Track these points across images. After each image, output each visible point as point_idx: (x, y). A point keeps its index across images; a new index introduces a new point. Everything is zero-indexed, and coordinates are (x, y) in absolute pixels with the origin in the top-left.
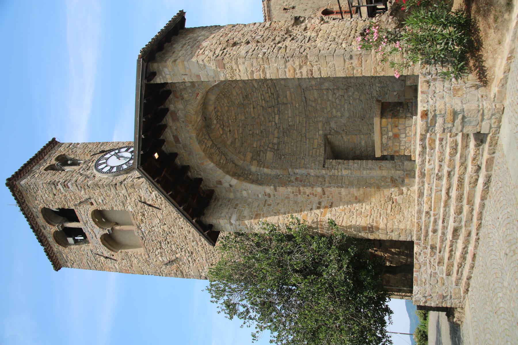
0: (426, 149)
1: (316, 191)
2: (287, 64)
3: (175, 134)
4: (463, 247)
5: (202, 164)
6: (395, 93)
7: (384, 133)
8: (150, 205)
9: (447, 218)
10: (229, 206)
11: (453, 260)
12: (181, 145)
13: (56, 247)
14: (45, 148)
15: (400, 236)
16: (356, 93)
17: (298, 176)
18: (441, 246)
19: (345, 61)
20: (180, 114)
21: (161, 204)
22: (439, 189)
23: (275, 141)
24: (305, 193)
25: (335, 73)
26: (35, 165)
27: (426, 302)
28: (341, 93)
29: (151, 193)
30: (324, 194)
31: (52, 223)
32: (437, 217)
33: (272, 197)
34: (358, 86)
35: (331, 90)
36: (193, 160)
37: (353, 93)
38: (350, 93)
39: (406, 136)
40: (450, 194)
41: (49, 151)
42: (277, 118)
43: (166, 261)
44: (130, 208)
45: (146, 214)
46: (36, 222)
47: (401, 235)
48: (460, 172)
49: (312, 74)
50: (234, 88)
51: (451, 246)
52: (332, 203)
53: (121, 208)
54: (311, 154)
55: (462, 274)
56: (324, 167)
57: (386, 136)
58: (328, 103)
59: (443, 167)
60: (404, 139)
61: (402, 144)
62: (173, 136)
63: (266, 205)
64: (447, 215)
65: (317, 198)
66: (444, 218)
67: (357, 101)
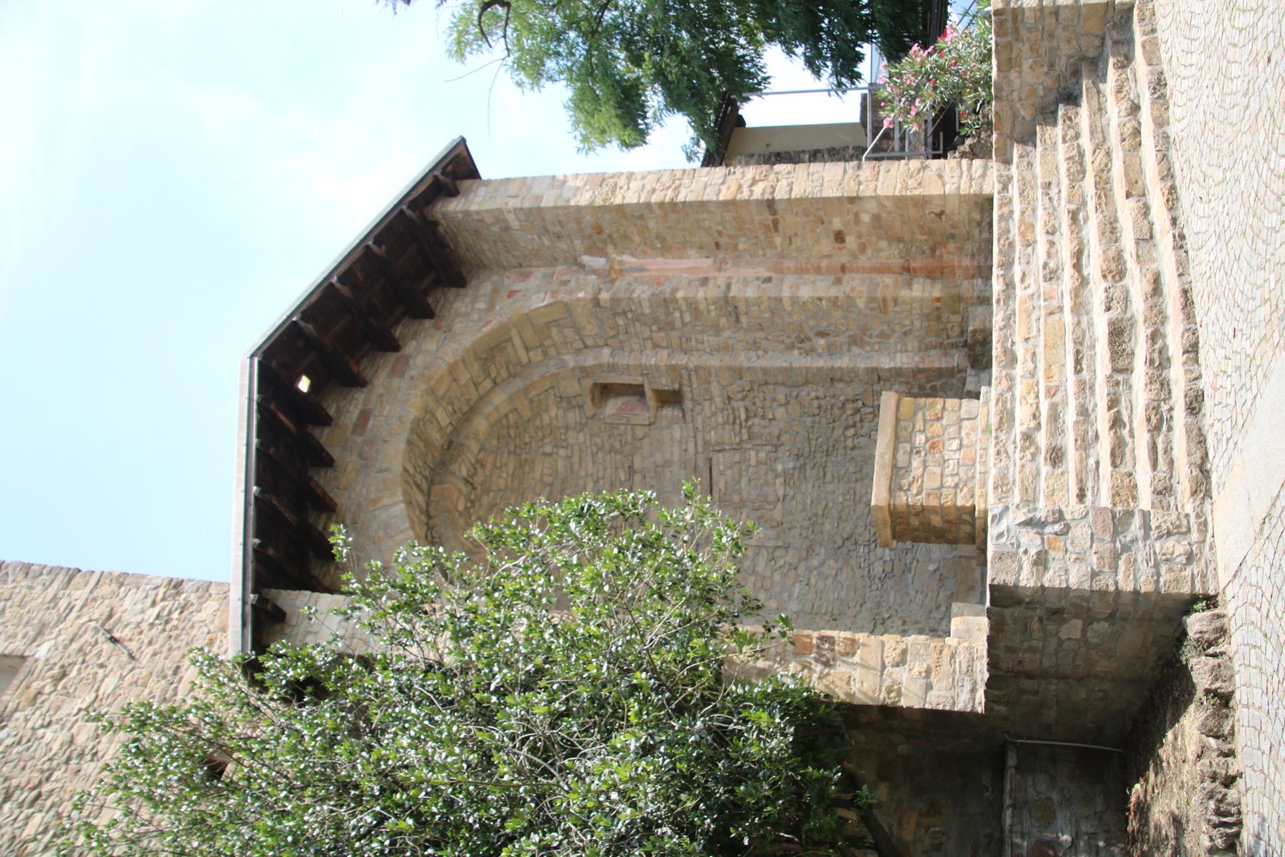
0: (1014, 288)
2: (729, 178)
3: (370, 406)
4: (1149, 331)
5: (375, 501)
6: (932, 567)
7: (902, 434)
9: (1085, 350)
11: (1129, 468)
12: (359, 439)
15: (929, 687)
16: (831, 562)
18: (1082, 461)
19: (845, 172)
20: (419, 361)
21: (150, 643)
22: (1055, 303)
25: (821, 191)
27: (1041, 561)
28: (791, 557)
29: (154, 604)
32: (1057, 399)
34: (839, 543)
35: (766, 547)
36: (358, 489)
37: (823, 563)
38: (815, 562)
39: (961, 446)
40: (1085, 273)
44: (42, 652)
45: (74, 673)
47: (933, 679)
48: (1096, 164)
49: (773, 193)
50: (545, 454)
51: (1113, 403)
53: (17, 646)
55: (1171, 463)
57: (908, 447)
58: (753, 578)
59: (1058, 246)
60: (957, 456)
61: (947, 471)
62: (362, 412)
64: (1087, 342)
66: (1078, 352)
67: (830, 581)
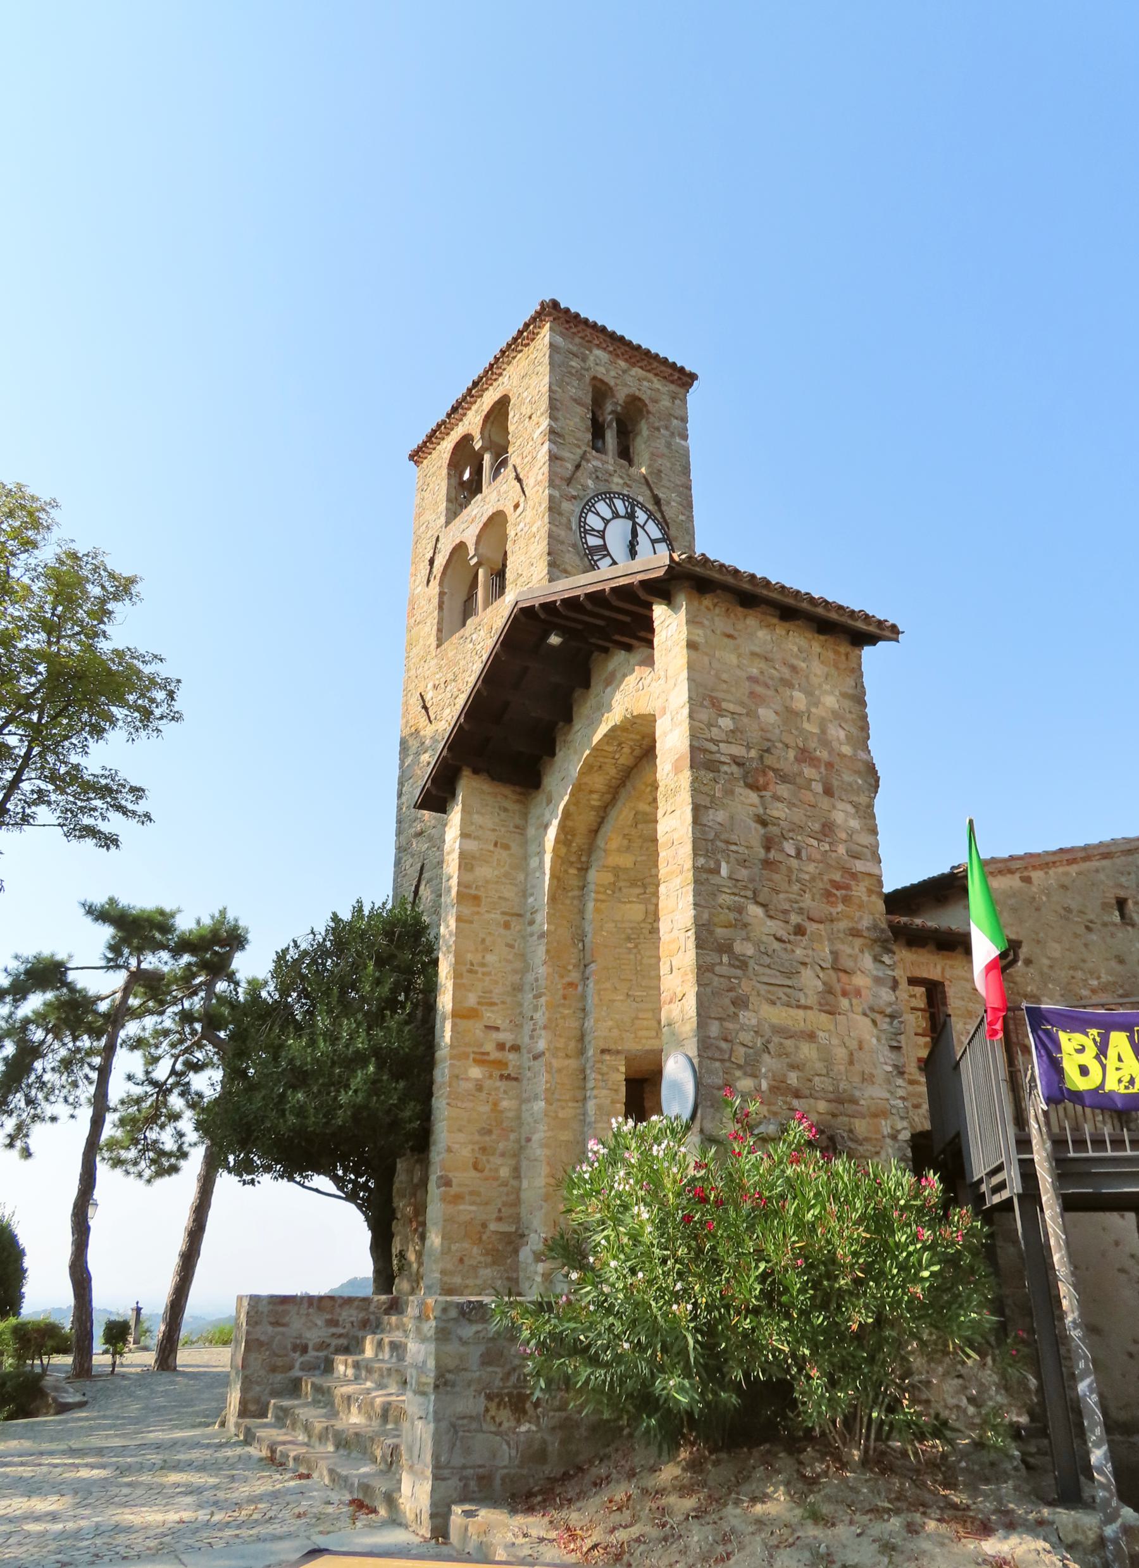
1: (539, 1037)
10: (503, 829)
17: (580, 988)
26: (610, 352)
31: (488, 425)
41: (656, 375)
46: (487, 389)
52: (516, 1079)
54: (641, 1015)
56: (603, 1051)
63: (508, 918)
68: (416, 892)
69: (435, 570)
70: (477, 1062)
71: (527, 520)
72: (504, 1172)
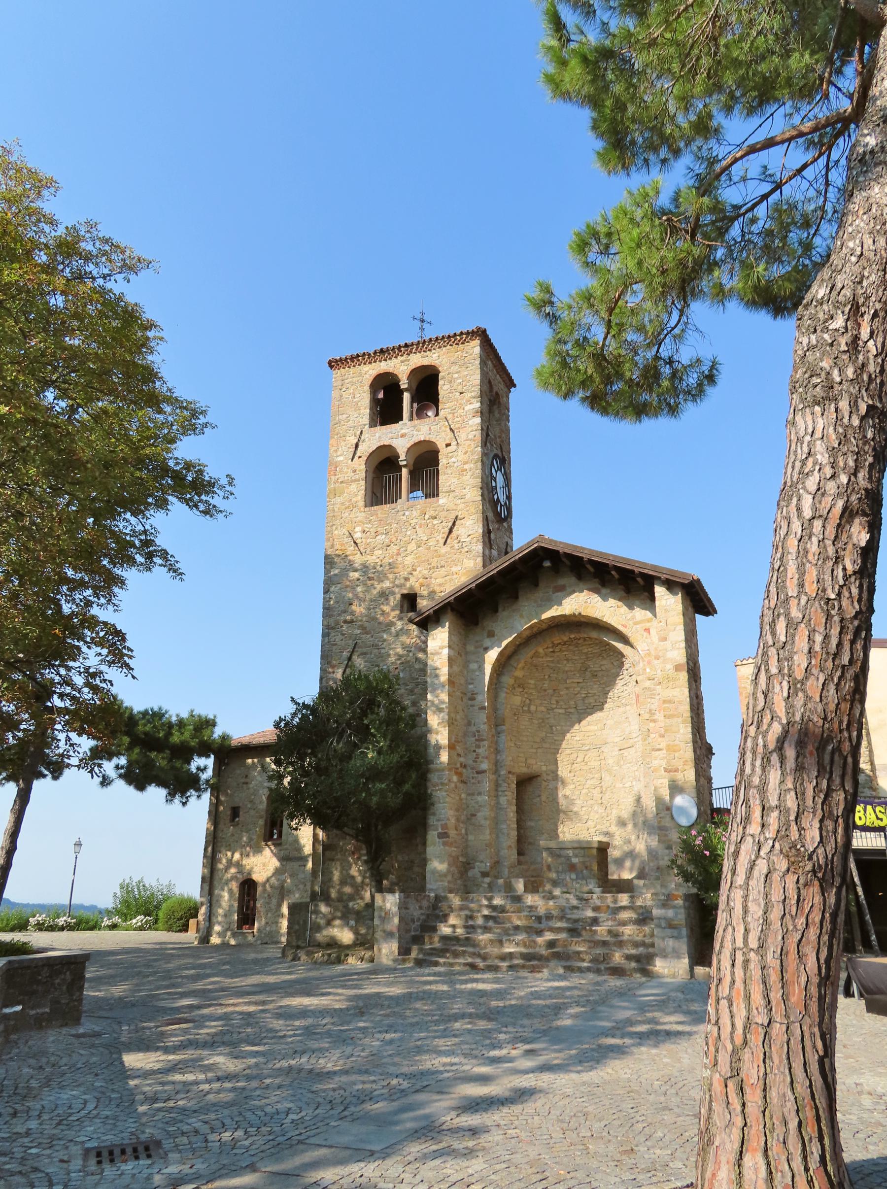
8: (451, 531)
13: (371, 371)
14: (508, 375)
23: (533, 708)
24: (479, 747)
30: (478, 773)
33: (470, 702)
39: (572, 880)
42: (561, 711)
43: (356, 536)
65: (470, 762)
68: (350, 659)
69: (358, 454)
70: (456, 773)
71: (460, 458)
72: (463, 831)
